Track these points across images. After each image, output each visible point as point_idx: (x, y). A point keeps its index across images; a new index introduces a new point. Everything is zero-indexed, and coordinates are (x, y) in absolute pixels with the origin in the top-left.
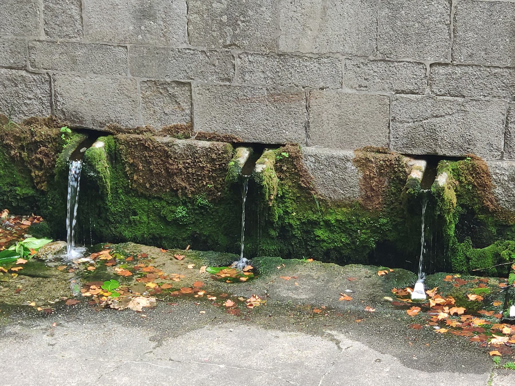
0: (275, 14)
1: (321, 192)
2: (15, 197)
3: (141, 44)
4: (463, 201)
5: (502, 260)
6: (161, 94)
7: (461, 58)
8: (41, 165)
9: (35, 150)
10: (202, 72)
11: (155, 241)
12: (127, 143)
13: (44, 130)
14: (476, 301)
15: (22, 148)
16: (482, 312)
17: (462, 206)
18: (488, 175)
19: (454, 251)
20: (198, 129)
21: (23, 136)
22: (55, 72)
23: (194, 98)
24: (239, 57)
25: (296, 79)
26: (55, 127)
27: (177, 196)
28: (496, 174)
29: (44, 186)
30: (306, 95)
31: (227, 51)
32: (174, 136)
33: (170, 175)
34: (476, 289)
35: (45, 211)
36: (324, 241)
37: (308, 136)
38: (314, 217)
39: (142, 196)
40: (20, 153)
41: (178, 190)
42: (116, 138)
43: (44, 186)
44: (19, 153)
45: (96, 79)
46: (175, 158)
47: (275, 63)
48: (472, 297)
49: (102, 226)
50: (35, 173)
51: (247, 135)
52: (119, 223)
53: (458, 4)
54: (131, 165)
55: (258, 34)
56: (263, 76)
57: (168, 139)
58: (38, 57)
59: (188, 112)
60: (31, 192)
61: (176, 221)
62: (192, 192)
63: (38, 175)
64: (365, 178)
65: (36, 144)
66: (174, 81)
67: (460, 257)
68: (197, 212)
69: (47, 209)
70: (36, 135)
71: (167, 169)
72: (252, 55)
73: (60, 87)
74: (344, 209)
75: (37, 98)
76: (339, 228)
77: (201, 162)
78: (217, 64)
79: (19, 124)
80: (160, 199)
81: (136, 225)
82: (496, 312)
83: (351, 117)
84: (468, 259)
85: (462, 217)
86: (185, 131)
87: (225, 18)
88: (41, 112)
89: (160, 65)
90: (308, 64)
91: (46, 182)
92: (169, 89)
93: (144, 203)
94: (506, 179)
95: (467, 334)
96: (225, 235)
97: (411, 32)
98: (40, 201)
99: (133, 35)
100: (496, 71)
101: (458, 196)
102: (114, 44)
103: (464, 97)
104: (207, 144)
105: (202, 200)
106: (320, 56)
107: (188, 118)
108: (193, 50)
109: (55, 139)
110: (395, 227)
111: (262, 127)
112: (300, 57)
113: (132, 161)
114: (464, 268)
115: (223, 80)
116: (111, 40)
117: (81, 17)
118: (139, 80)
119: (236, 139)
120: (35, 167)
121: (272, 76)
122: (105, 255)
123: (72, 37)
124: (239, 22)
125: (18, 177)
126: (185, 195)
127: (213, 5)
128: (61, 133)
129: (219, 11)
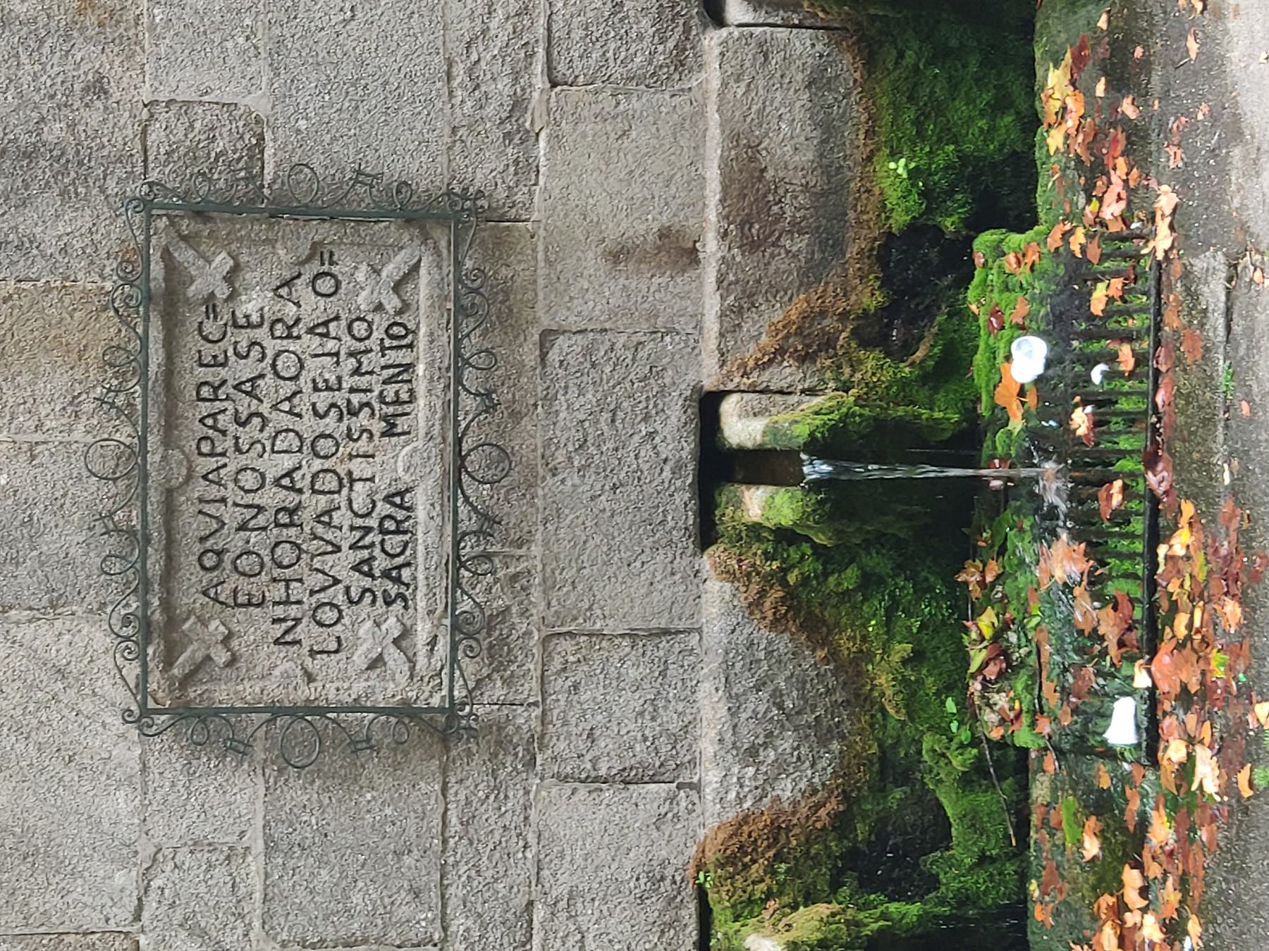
4: (822, 885)
5: (979, 768)
14: (1101, 835)
16: (1131, 819)
17: (835, 885)
18: (745, 820)
19: (964, 899)
28: (740, 800)
34: (1067, 835)
48: (1092, 847)
53: (274, 939)
67: (979, 881)
82: (1126, 779)
84: (983, 860)
85: (868, 883)
94: (751, 771)
95: (1199, 861)
100: (454, 820)
101: (810, 899)
114: (1010, 868)
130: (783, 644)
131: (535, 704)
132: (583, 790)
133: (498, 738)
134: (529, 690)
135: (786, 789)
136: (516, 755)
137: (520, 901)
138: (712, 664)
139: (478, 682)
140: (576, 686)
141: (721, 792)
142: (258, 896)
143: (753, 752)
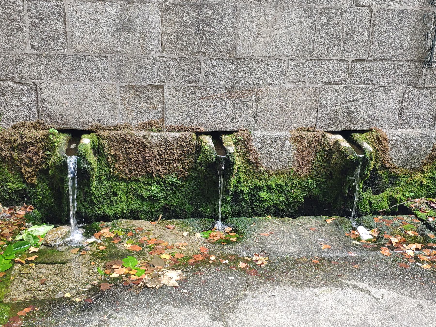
0: (235, 24)
1: (264, 165)
2: (7, 192)
3: (121, 53)
6: (138, 96)
7: (375, 55)
8: (31, 162)
9: (24, 150)
10: (173, 76)
11: (134, 215)
12: (109, 138)
13: (33, 133)
15: (13, 149)
20: (168, 123)
21: (13, 139)
22: (41, 81)
23: (166, 98)
24: (205, 63)
25: (249, 78)
26: (42, 129)
27: (152, 177)
29: (34, 180)
30: (256, 92)
31: (194, 58)
32: (149, 130)
33: (146, 161)
35: (35, 201)
36: (266, 200)
37: (256, 123)
38: (260, 184)
39: (124, 180)
40: (11, 154)
41: (153, 173)
42: (99, 135)
43: (34, 180)
44: (10, 153)
45: (79, 86)
46: (151, 148)
47: (232, 66)
49: (87, 208)
50: (25, 169)
51: (208, 126)
52: (102, 203)
53: (377, 12)
54: (113, 156)
55: (221, 42)
56: (223, 77)
57: (144, 133)
58: (24, 69)
59: (160, 110)
60: (21, 186)
61: (151, 199)
62: (165, 174)
63: (28, 171)
64: (298, 152)
65: (26, 145)
66: (149, 85)
68: (168, 188)
69: (37, 198)
70: (25, 137)
71: (144, 158)
72: (215, 60)
73: (46, 94)
74: (282, 176)
75: (24, 105)
76: (277, 190)
77: (172, 149)
78: (186, 69)
79: (8, 129)
80: (137, 181)
81: (117, 204)
83: (289, 106)
86: (159, 125)
87: (193, 30)
88: (28, 117)
89: (137, 71)
90: (259, 65)
91: (35, 177)
92: (144, 91)
93: (124, 185)
96: (191, 204)
97: (340, 36)
98: (30, 192)
99: (113, 46)
100: (399, 63)
102: (96, 55)
103: (374, 84)
104: (177, 135)
105: (173, 179)
106: (269, 58)
107: (160, 115)
108: (166, 58)
109: (43, 140)
110: (319, 185)
111: (220, 118)
112: (254, 60)
113: (114, 153)
115: (190, 82)
116: (93, 51)
117: (66, 32)
118: (118, 85)
119: (199, 129)
120: (26, 164)
121: (230, 77)
122: (106, 232)
123: (57, 50)
124: (206, 33)
125: (9, 174)
126: (159, 176)
127: (185, 18)
128: (49, 134)
129: (188, 23)
130: (429, 151)
131: (424, 86)
132: (400, 99)
133: (417, 76)
134: (428, 84)
135: (393, 152)
136: (413, 80)
137: (375, 81)
138: (426, 133)
139: (433, 70)
140: (426, 97)
141: (394, 134)
142: (389, 7)
143: (404, 143)
